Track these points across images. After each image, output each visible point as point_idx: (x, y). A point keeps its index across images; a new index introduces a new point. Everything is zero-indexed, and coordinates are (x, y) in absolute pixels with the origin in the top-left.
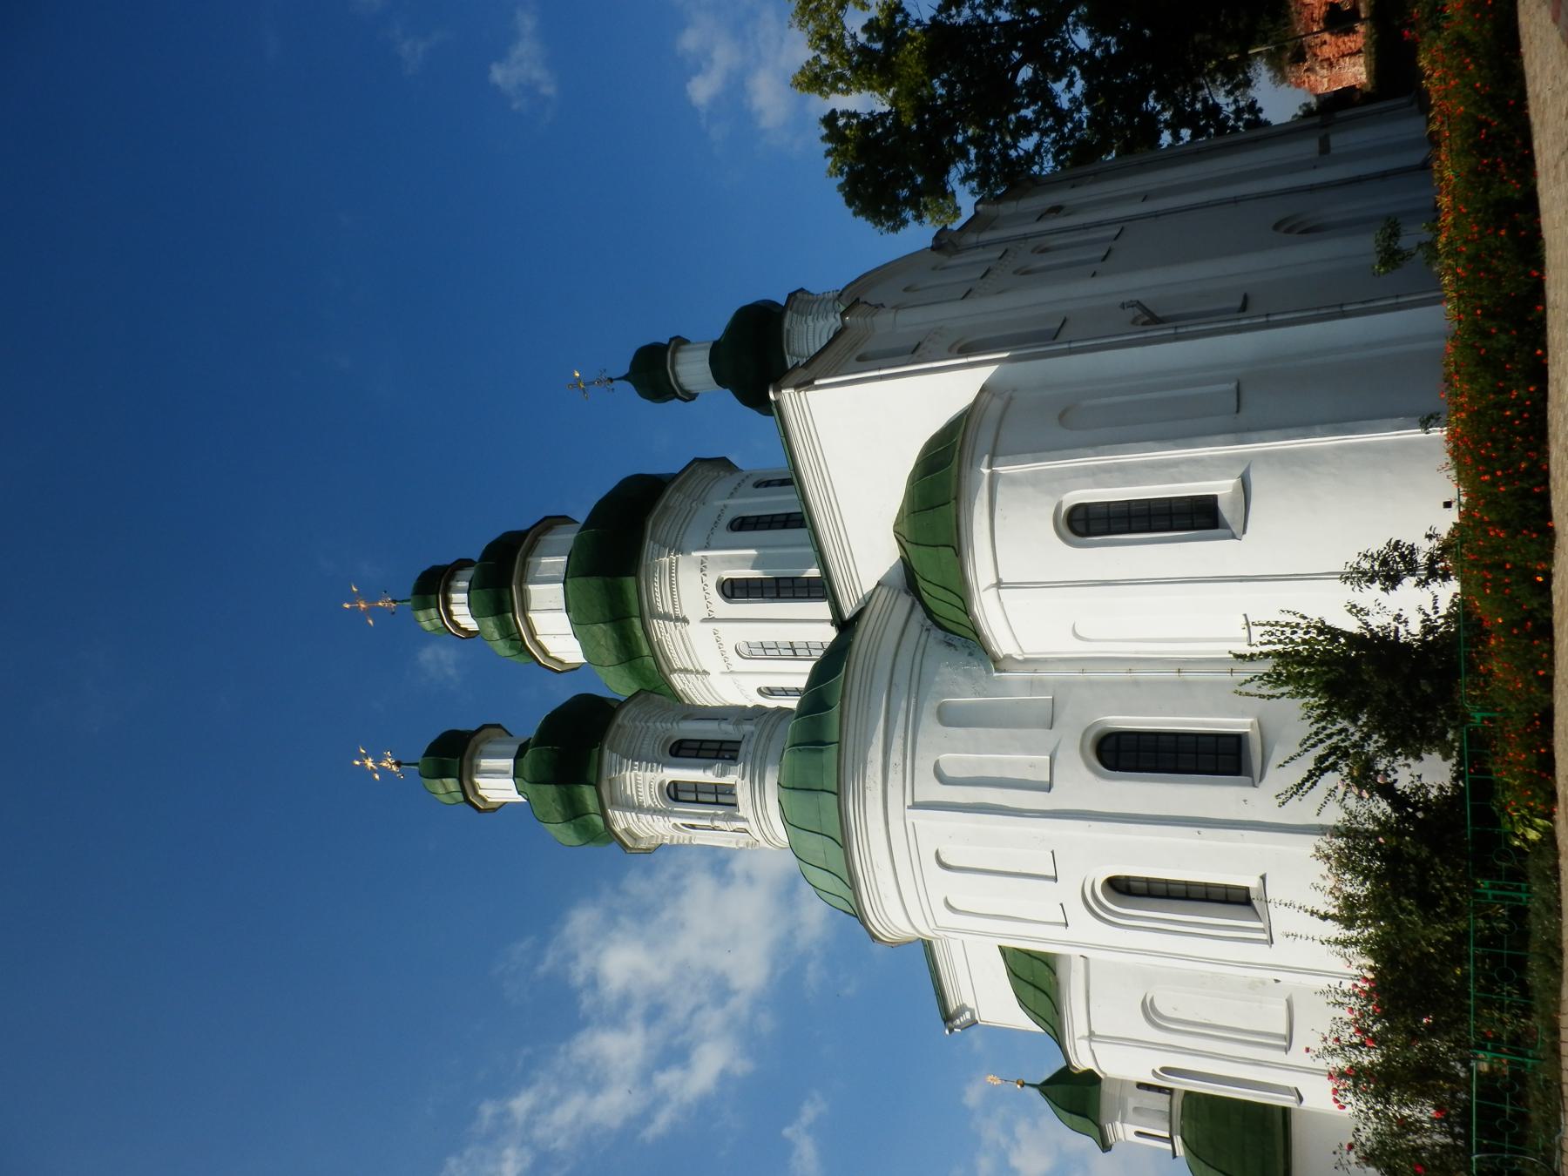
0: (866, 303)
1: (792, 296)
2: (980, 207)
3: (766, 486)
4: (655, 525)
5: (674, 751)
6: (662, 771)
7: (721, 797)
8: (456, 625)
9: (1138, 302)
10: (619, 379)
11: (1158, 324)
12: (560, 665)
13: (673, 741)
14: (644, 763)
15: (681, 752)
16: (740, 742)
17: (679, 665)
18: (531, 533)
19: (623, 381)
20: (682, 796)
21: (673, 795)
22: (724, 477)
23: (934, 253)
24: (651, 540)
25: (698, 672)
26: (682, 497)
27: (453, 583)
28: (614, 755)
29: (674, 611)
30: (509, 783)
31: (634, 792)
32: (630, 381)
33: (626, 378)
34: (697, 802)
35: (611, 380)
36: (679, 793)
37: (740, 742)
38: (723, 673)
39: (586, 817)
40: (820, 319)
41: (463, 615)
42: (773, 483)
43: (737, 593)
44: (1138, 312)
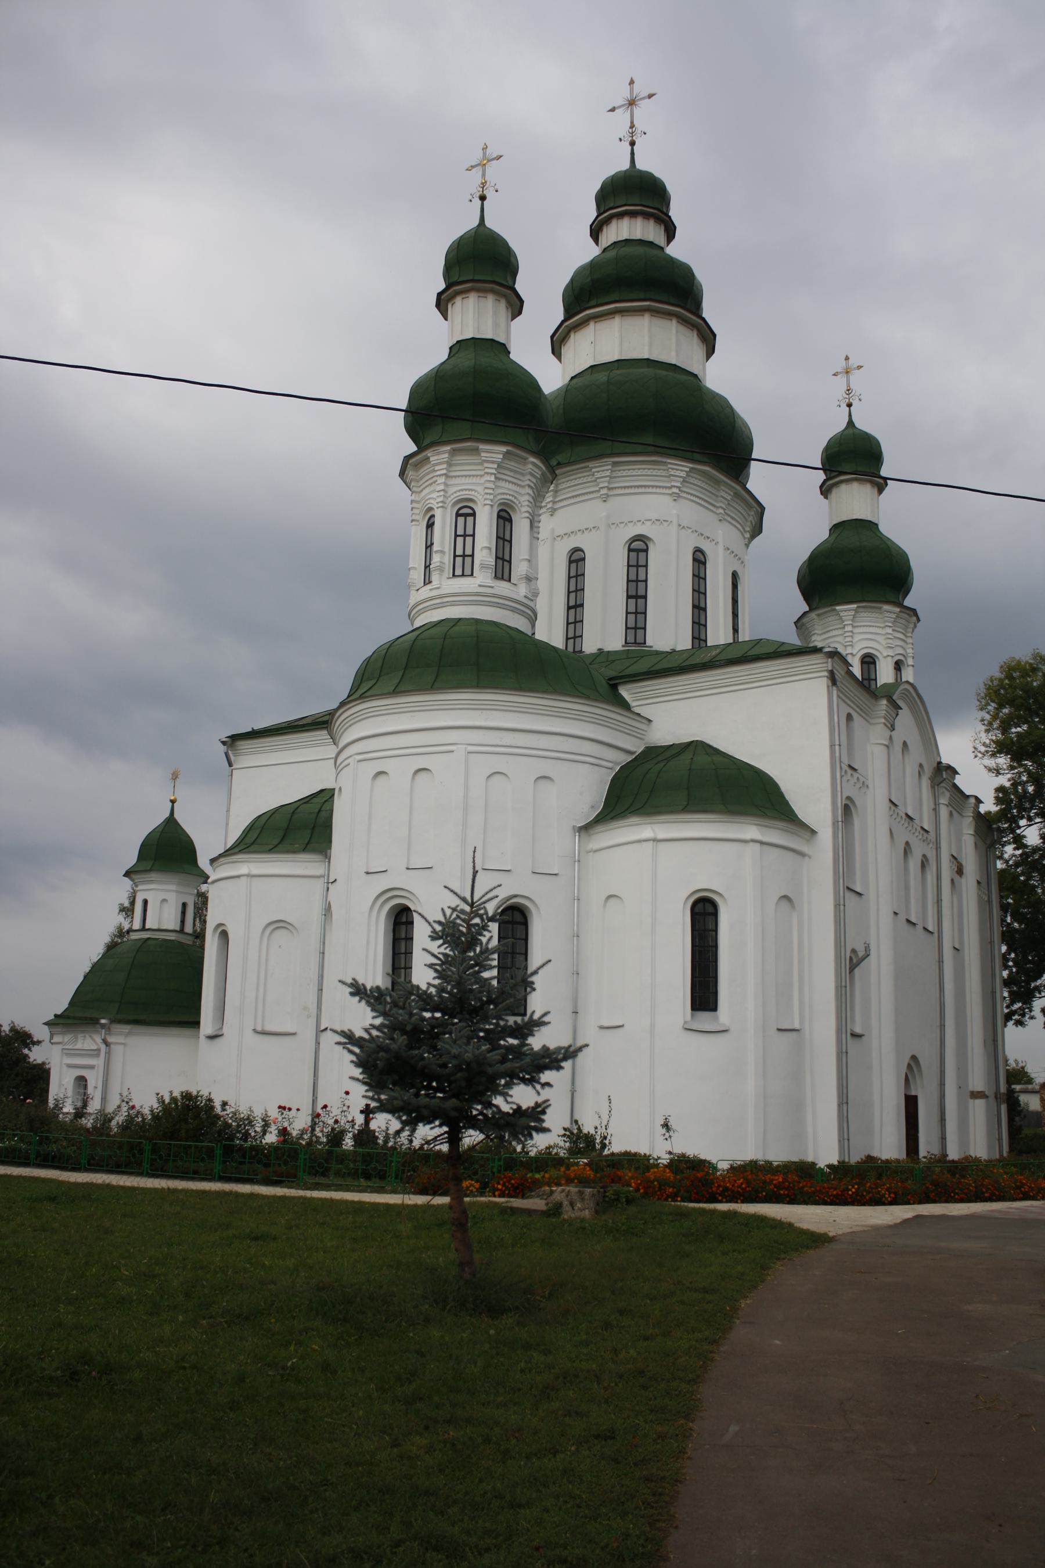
0: (897, 715)
1: (914, 612)
2: (973, 800)
4: (704, 473)
5: (503, 514)
9: (868, 955)
10: (850, 415)
11: (850, 968)
13: (511, 513)
18: (701, 322)
19: (847, 419)
22: (745, 538)
24: (692, 468)
26: (729, 498)
28: (501, 456)
32: (846, 428)
33: (851, 423)
35: (849, 405)
36: (463, 518)
37: (509, 580)
43: (633, 555)
44: (861, 954)
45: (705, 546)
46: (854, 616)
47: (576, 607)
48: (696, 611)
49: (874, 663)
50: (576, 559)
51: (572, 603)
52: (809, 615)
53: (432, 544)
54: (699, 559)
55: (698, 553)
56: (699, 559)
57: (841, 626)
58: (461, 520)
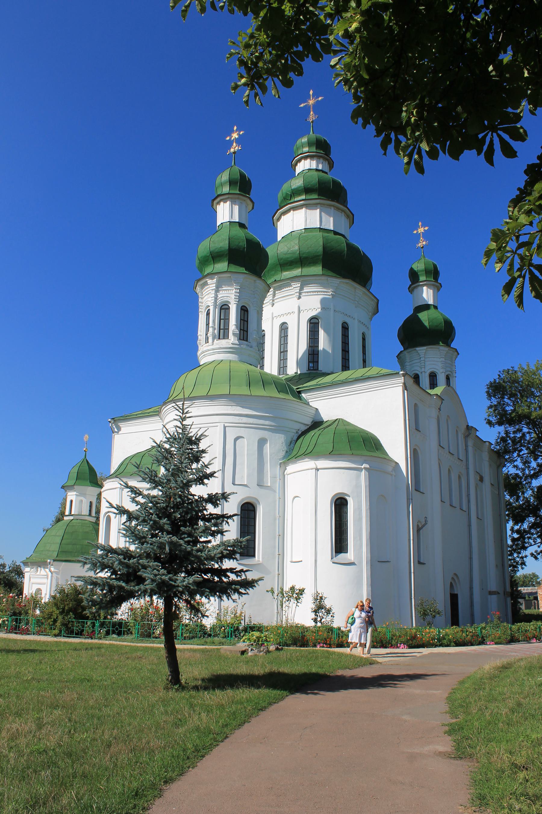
0: (442, 403)
2: (487, 444)
3: (363, 338)
4: (347, 283)
6: (235, 304)
7: (223, 333)
8: (299, 161)
12: (277, 218)
14: (238, 295)
15: (243, 311)
16: (247, 341)
17: (276, 292)
18: (346, 209)
20: (223, 311)
21: (223, 307)
23: (466, 427)
25: (273, 301)
27: (321, 160)
29: (304, 292)
30: (227, 219)
31: (224, 288)
34: (220, 319)
37: (247, 341)
38: (273, 313)
39: (212, 262)
40: (442, 365)
41: (303, 166)
42: (364, 355)
45: (348, 321)
46: (425, 353)
47: (284, 352)
48: (344, 352)
49: (436, 376)
50: (284, 328)
51: (282, 350)
52: (403, 352)
53: (209, 323)
54: (345, 328)
55: (345, 324)
56: (345, 328)
57: (419, 358)
58: (223, 311)
